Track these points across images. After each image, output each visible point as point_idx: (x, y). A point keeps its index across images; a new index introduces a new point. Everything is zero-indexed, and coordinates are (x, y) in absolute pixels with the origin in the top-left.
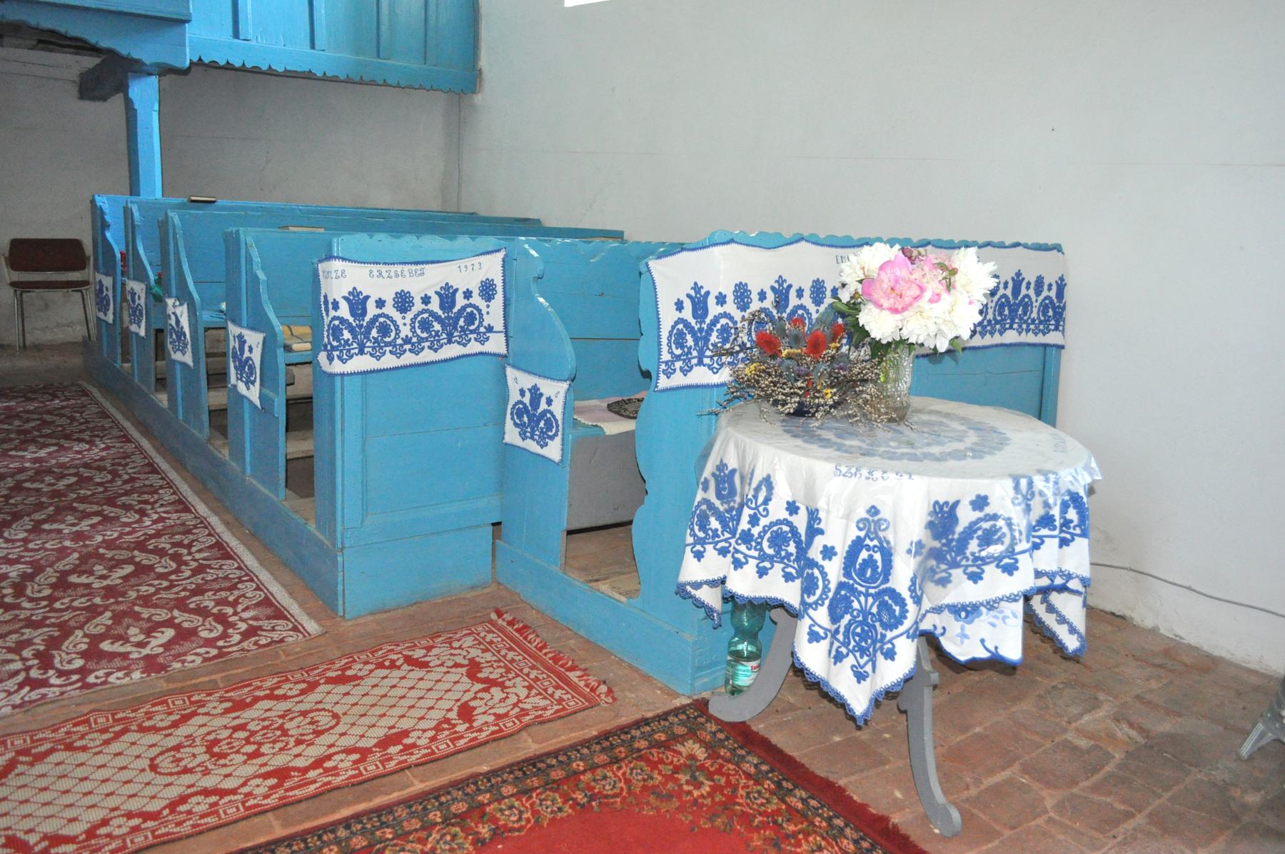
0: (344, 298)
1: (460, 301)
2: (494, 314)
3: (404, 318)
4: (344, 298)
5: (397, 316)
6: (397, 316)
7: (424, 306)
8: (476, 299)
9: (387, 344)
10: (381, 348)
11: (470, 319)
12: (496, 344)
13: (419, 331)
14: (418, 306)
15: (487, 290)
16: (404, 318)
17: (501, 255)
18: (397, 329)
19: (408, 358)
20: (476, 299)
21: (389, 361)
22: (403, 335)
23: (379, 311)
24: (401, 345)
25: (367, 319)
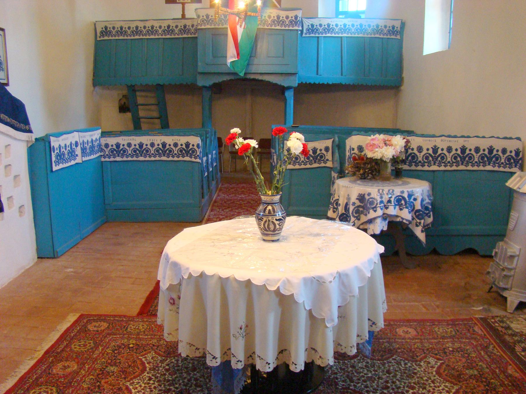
1: (318, 152)
2: (329, 156)
8: (323, 152)
11: (321, 157)
12: (329, 164)
15: (327, 149)
17: (331, 140)
19: (303, 166)
20: (323, 152)
21: (297, 167)
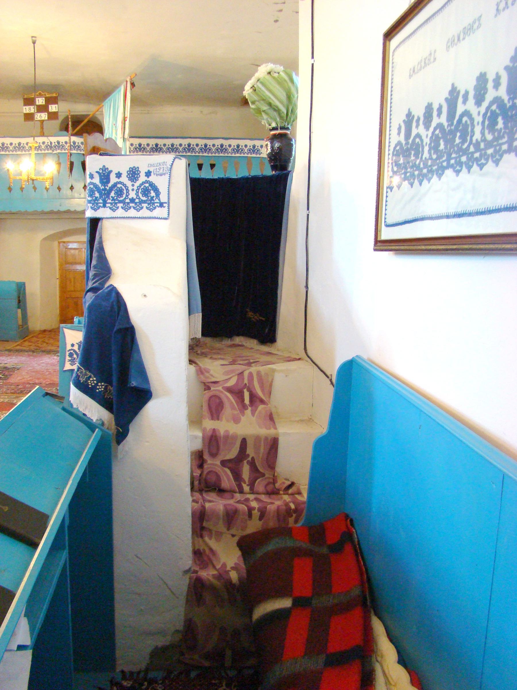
0: (97, 172)
3: (133, 185)
4: (97, 172)
5: (129, 184)
6: (129, 184)
7: (146, 178)
9: (120, 202)
10: (116, 203)
13: (140, 195)
14: (143, 178)
16: (133, 185)
18: (128, 192)
22: (130, 197)
23: (117, 180)
24: (128, 203)
25: (110, 185)
